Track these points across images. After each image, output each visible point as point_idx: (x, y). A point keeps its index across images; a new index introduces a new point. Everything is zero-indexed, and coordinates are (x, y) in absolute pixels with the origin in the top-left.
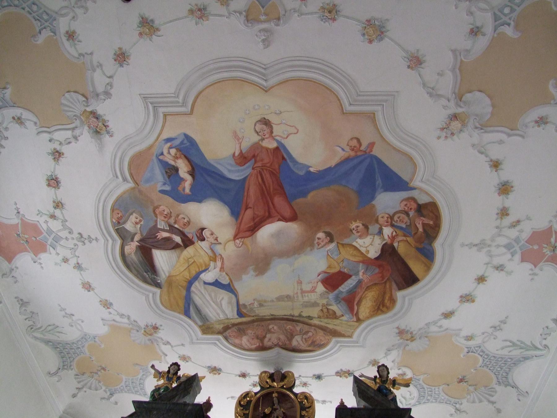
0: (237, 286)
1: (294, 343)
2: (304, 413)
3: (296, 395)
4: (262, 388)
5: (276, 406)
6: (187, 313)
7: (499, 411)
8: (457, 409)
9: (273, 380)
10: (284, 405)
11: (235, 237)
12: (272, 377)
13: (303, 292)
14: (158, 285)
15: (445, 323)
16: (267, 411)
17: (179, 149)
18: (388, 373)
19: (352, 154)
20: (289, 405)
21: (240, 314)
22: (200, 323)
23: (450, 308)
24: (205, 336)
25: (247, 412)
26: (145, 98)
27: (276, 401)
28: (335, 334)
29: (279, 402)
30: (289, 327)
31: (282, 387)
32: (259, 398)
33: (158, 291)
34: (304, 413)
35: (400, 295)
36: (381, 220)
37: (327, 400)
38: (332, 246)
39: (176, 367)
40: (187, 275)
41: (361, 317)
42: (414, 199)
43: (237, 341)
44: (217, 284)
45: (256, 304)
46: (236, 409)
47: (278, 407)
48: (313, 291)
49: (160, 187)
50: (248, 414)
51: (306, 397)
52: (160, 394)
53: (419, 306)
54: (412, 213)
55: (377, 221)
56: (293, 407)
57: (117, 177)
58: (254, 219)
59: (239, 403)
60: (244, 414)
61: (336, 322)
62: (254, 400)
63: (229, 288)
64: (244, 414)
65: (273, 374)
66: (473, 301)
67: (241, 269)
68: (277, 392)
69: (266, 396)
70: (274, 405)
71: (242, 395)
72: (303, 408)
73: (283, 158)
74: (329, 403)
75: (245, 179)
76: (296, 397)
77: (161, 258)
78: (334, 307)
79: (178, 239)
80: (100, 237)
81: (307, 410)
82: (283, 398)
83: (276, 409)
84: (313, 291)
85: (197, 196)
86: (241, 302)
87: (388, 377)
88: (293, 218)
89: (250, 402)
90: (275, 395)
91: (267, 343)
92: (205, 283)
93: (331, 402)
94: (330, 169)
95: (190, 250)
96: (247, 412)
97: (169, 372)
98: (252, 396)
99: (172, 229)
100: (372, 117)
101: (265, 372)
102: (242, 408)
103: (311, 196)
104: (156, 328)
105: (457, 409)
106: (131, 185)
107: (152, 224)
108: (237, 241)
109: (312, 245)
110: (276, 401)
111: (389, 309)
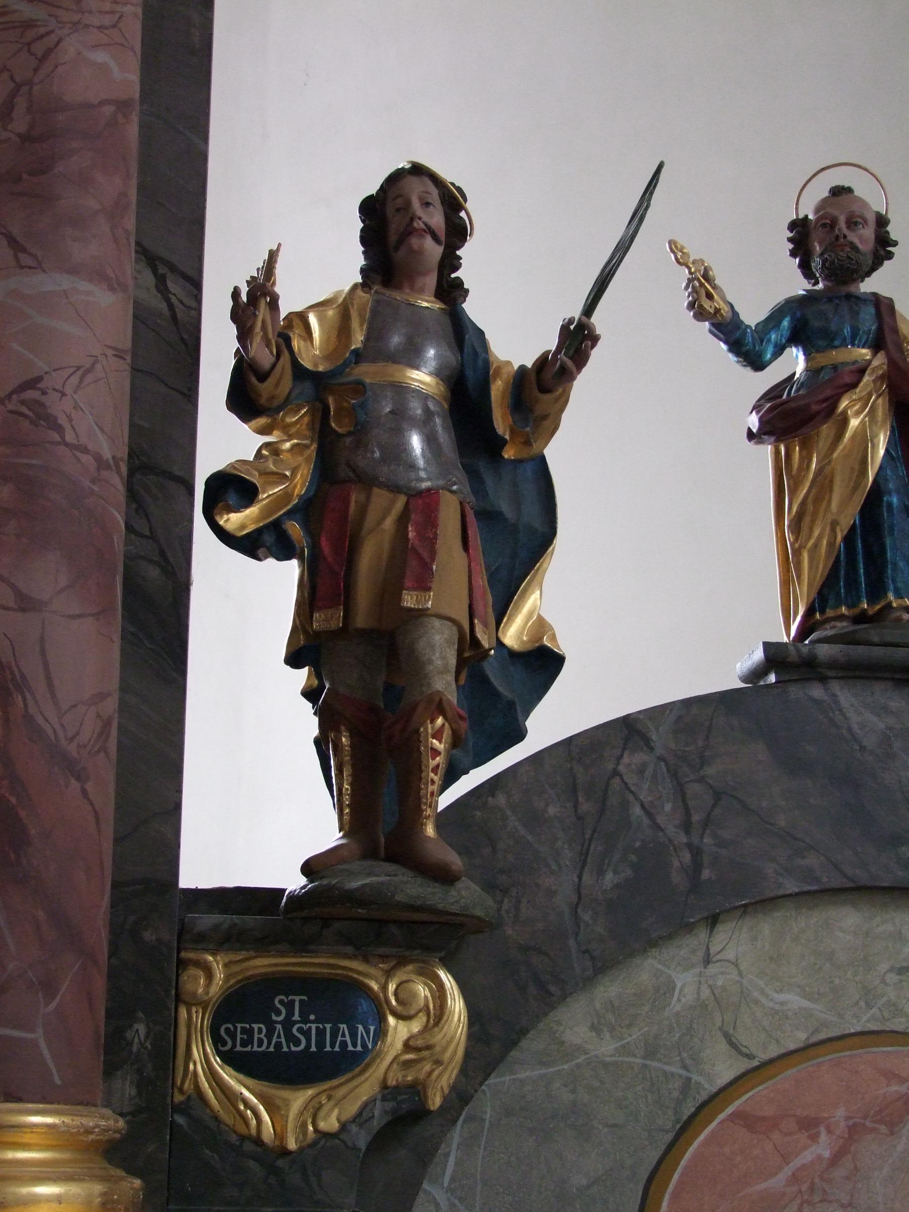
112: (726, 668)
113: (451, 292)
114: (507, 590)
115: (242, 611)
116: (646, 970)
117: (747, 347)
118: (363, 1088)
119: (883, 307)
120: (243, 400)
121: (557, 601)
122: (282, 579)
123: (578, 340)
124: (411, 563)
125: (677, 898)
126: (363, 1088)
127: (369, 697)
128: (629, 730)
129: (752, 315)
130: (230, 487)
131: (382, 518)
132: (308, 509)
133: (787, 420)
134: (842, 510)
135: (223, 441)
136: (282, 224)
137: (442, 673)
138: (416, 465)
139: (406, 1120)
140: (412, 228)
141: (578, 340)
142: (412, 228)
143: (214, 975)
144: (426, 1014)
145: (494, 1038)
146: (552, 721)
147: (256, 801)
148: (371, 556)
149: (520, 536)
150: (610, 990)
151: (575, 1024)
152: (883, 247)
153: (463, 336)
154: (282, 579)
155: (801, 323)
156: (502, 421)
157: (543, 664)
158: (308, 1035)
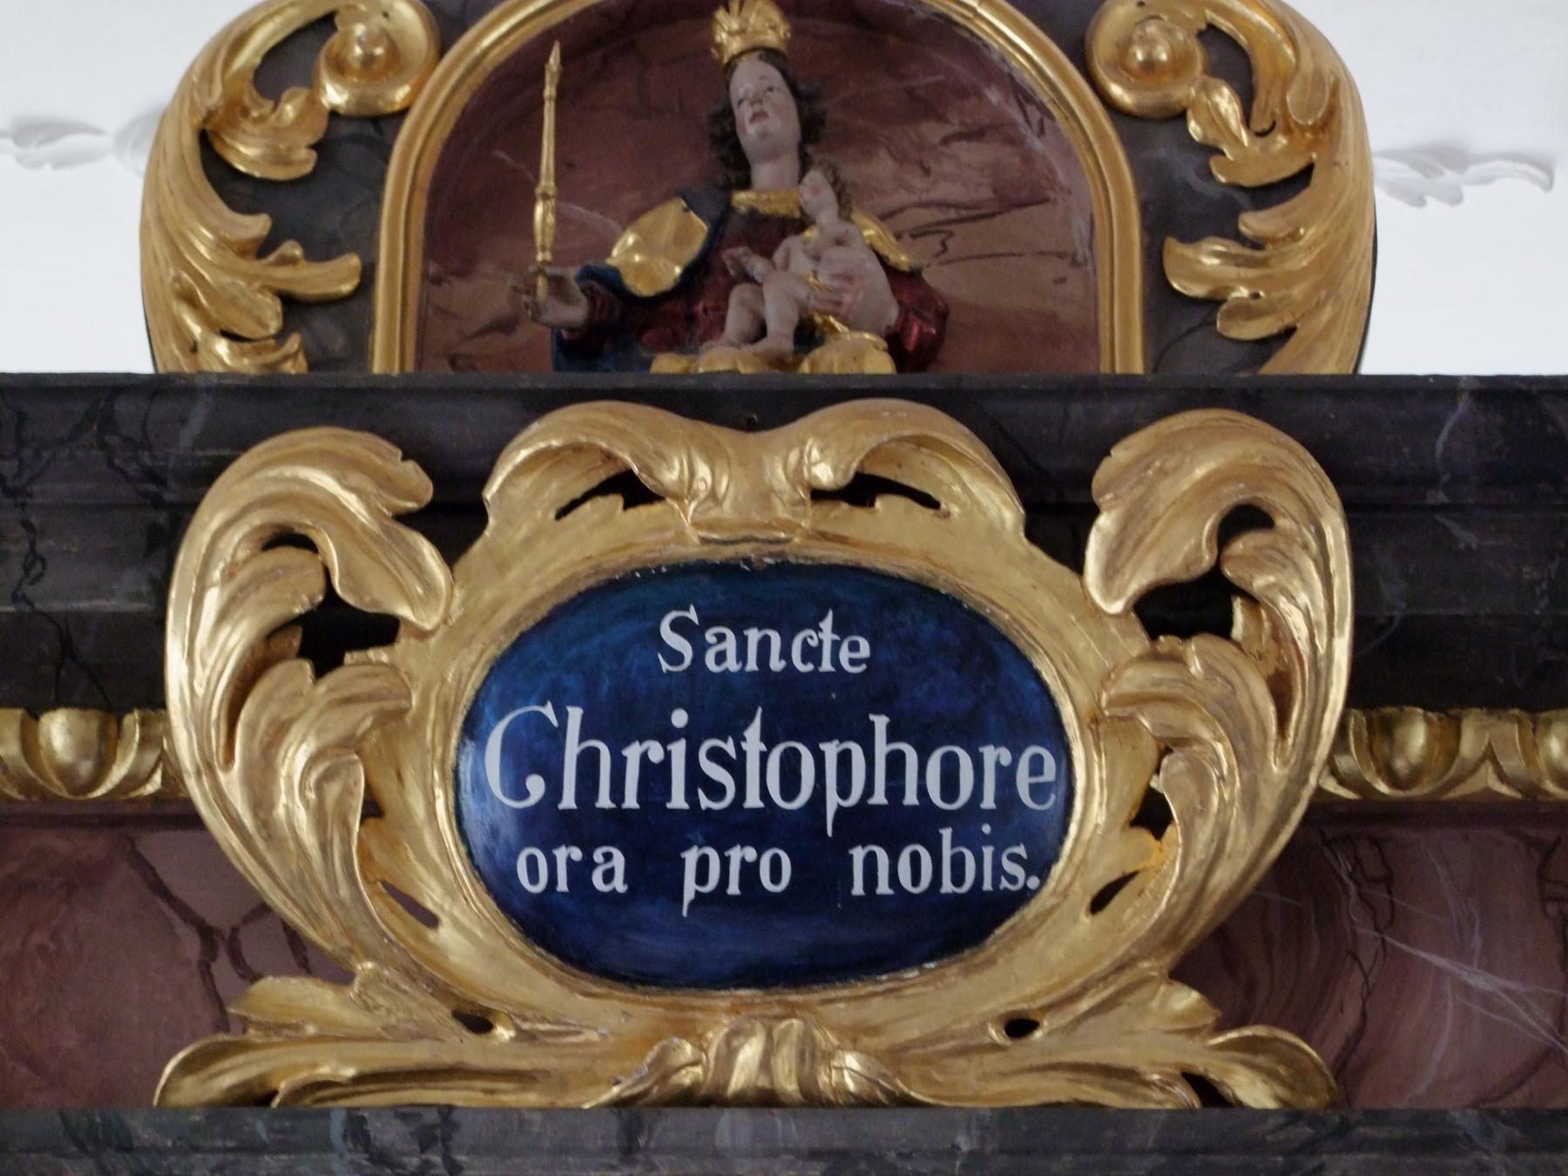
2: (1203, 264)
5: (769, 187)
10: (882, 167)
16: (650, 251)
20: (963, 171)
25: (339, 276)
27: (763, 110)
29: (812, 130)
32: (514, 80)
34: (1203, 264)
37: (1482, 139)
46: (162, 233)
47: (816, 193)
56: (1022, 193)
60: (294, 306)
62: (426, 104)
64: (294, 306)
70: (738, 169)
71: (236, 39)
72: (1185, 204)
74: (1517, 188)
76: (1080, 55)
81: (1252, 222)
83: (768, 233)
89: (359, 140)
93: (1543, 168)
96: (339, 276)
98: (394, 61)
102: (257, 225)
110: (763, 110)
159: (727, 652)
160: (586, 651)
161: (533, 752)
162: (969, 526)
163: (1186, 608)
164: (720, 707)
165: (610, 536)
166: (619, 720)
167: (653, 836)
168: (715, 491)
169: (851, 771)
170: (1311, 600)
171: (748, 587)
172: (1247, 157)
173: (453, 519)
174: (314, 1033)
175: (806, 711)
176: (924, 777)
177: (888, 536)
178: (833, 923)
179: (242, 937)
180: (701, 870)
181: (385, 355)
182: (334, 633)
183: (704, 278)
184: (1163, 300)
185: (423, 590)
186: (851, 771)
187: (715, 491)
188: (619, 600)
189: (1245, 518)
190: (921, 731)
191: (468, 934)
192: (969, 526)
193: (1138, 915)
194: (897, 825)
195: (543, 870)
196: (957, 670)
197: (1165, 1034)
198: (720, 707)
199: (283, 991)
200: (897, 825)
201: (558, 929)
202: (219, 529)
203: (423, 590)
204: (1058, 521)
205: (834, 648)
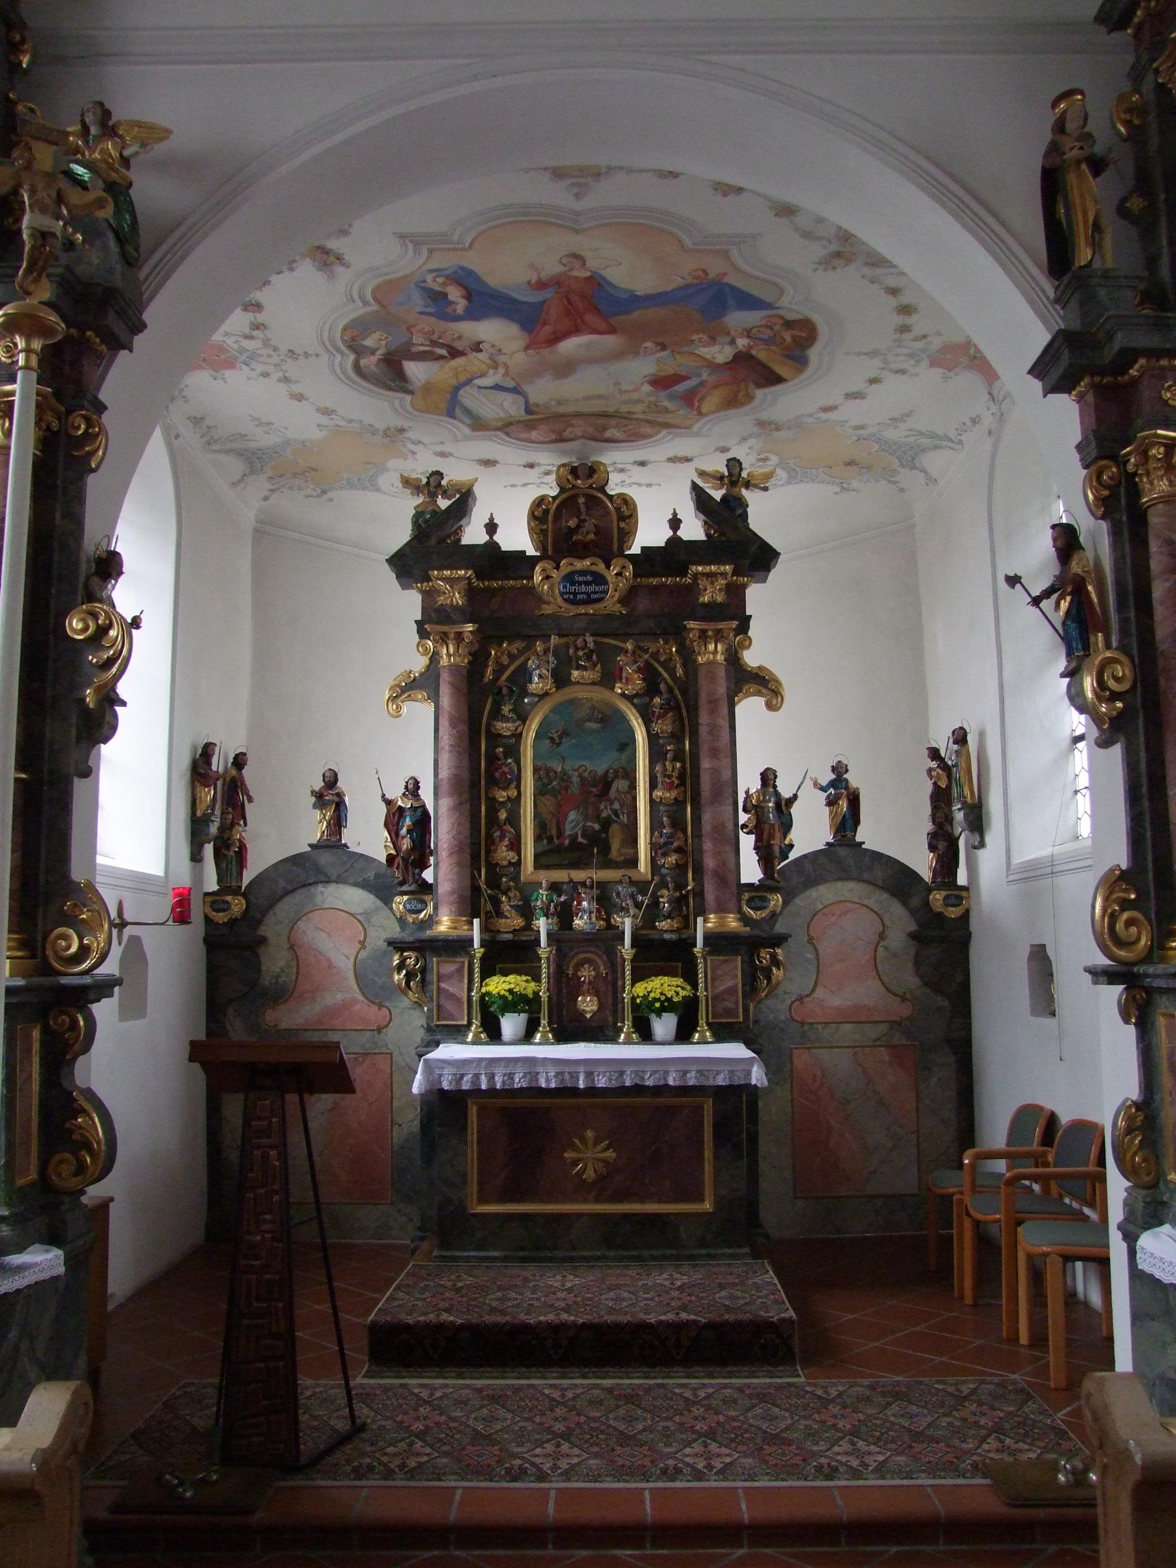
0: (527, 388)
1: (608, 434)
2: (622, 525)
3: (610, 497)
4: (562, 490)
6: (451, 414)
7: (902, 490)
8: (843, 488)
9: (577, 477)
11: (527, 348)
12: (574, 471)
13: (621, 392)
14: (411, 392)
15: (824, 416)
16: (572, 523)
17: (447, 277)
18: (741, 469)
19: (696, 281)
21: (528, 411)
22: (468, 421)
23: (830, 403)
24: (475, 433)
26: (402, 237)
28: (667, 425)
30: (601, 421)
31: (591, 487)
33: (408, 398)
34: (622, 525)
35: (760, 393)
36: (733, 333)
38: (664, 354)
39: (438, 477)
40: (454, 382)
41: (704, 410)
42: (781, 317)
43: (524, 435)
44: (497, 387)
45: (553, 403)
46: (529, 523)
48: (636, 390)
49: (419, 309)
50: (546, 530)
51: (626, 500)
52: (426, 522)
53: (787, 402)
54: (776, 328)
55: (728, 333)
57: (354, 301)
58: (554, 333)
59: (532, 516)
61: (669, 415)
63: (515, 390)
65: (576, 468)
66: (864, 398)
67: (534, 373)
68: (584, 495)
69: (568, 502)
72: (622, 518)
73: (599, 284)
75: (544, 302)
77: (415, 370)
78: (666, 404)
79: (443, 352)
80: (321, 350)
82: (594, 502)
83: (585, 520)
84: (636, 390)
85: (474, 314)
86: (531, 401)
87: (740, 474)
88: (612, 330)
89: (546, 512)
90: (581, 500)
91: (566, 435)
92: (480, 387)
94: (665, 293)
95: (460, 361)
97: (428, 483)
99: (433, 343)
100: (726, 254)
101: (564, 465)
103: (635, 315)
104: (402, 430)
105: (843, 488)
106: (375, 307)
107: (405, 339)
108: (531, 351)
109: (637, 353)
111: (742, 404)
112: (821, 846)
113: (775, 787)
114: (785, 835)
115: (747, 842)
116: (807, 893)
117: (823, 789)
118: (767, 911)
119: (846, 780)
120: (745, 810)
121: (794, 836)
122: (752, 838)
123: (795, 797)
124: (771, 836)
125: (812, 882)
126: (767, 911)
127: (766, 856)
128: (805, 856)
129: (824, 784)
130: (744, 826)
131: (766, 827)
132: (755, 827)
133: (831, 802)
134: (839, 818)
135: (743, 818)
136: (748, 782)
137: (777, 850)
138: (771, 817)
139: (774, 915)
140: (768, 778)
141: (795, 797)
142: (768, 778)
143: (746, 896)
144: (776, 900)
145: (786, 903)
146: (793, 855)
147: (751, 871)
148: (766, 834)
149: (787, 826)
150: (802, 896)
151: (799, 901)
152: (847, 771)
153: (777, 794)
154: (753, 837)
155: (832, 784)
156: (784, 806)
157: (791, 846)
158: (759, 904)
159: (581, 579)
160: (569, 578)
161: (565, 587)
162: (601, 567)
163: (619, 574)
164: (580, 583)
165: (570, 568)
166: (573, 583)
167: (575, 594)
168: (580, 565)
169: (590, 589)
170: (629, 573)
171: (583, 573)
172: (627, 513)
173: (558, 568)
174: (547, 610)
175: (587, 583)
176: (597, 589)
177: (594, 568)
178: (589, 601)
179: (540, 600)
180: (579, 597)
181: (550, 553)
182: (548, 577)
183: (578, 526)
184: (619, 528)
185: (555, 573)
186: (590, 589)
187: (580, 565)
188: (573, 573)
189: (624, 567)
190: (597, 585)
191: (560, 600)
192: (601, 567)
193: (616, 598)
194: (595, 593)
195: (566, 596)
196: (599, 579)
197: (618, 608)
198: (580, 583)
199: (544, 606)
200: (595, 593)
201: (566, 600)
202: (538, 569)
203: (555, 573)
204: (608, 567)
205: (589, 578)
